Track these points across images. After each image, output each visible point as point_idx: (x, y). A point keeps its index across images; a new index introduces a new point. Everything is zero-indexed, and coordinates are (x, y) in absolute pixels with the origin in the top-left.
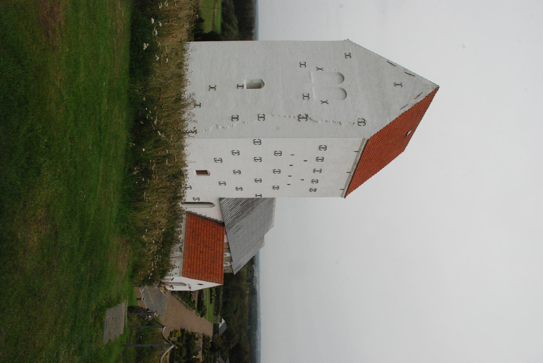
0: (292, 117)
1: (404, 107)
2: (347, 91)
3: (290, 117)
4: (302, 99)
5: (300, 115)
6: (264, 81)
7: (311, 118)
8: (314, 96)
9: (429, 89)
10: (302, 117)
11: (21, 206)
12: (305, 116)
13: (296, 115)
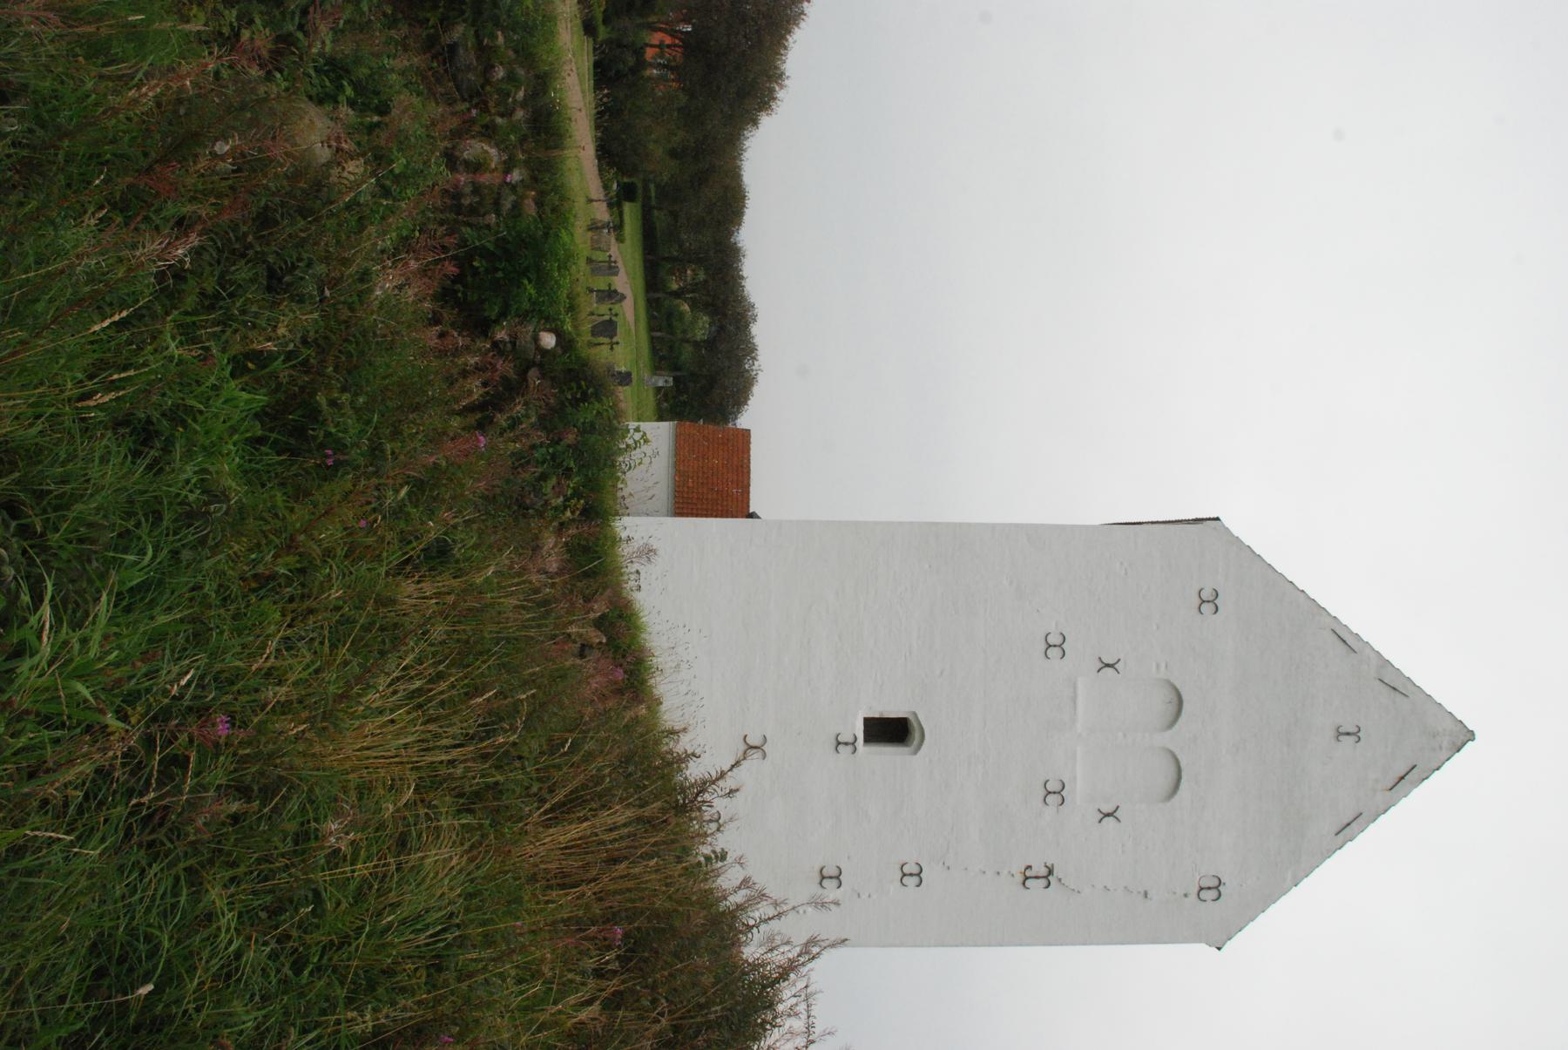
0: (1005, 872)
1: (1348, 824)
2: (1184, 698)
3: (998, 873)
4: (1041, 804)
5: (1029, 867)
6: (924, 726)
7: (1060, 880)
8: (1078, 792)
9: (1441, 748)
10: (1033, 875)
11: (384, 518)
12: (1044, 871)
13: (1017, 868)
